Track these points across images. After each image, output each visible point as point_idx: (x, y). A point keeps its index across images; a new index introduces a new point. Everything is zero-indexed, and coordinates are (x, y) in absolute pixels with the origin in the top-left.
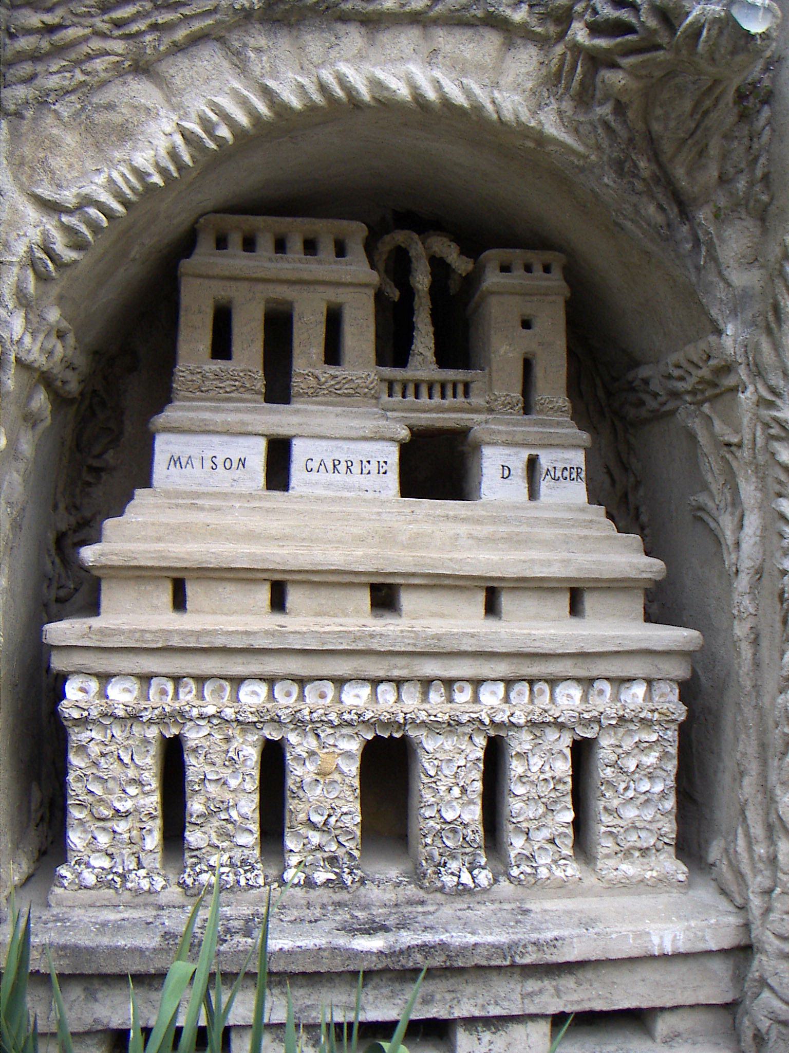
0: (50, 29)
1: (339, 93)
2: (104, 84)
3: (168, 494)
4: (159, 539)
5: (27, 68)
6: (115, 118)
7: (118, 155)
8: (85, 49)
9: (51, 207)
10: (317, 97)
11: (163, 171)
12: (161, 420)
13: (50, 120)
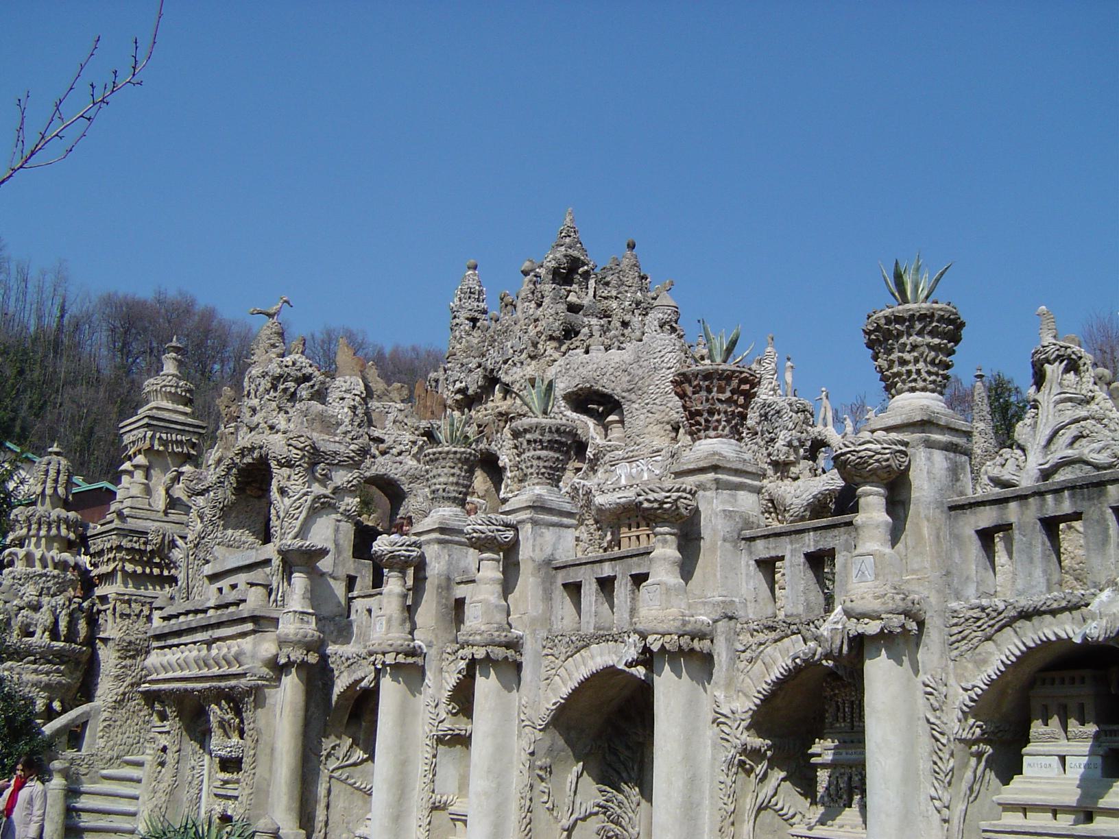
0: (960, 632)
1: (1045, 639)
2: (977, 647)
3: (1027, 777)
4: (1017, 794)
5: (956, 645)
6: (981, 657)
7: (983, 669)
8: (971, 636)
9: (966, 690)
10: (1039, 642)
11: (996, 674)
12: (1024, 750)
13: (964, 660)
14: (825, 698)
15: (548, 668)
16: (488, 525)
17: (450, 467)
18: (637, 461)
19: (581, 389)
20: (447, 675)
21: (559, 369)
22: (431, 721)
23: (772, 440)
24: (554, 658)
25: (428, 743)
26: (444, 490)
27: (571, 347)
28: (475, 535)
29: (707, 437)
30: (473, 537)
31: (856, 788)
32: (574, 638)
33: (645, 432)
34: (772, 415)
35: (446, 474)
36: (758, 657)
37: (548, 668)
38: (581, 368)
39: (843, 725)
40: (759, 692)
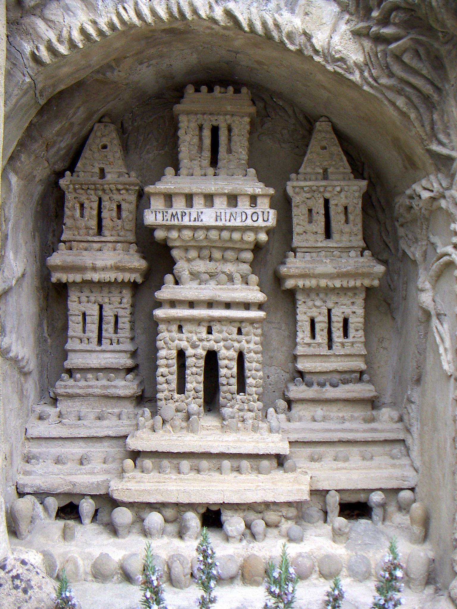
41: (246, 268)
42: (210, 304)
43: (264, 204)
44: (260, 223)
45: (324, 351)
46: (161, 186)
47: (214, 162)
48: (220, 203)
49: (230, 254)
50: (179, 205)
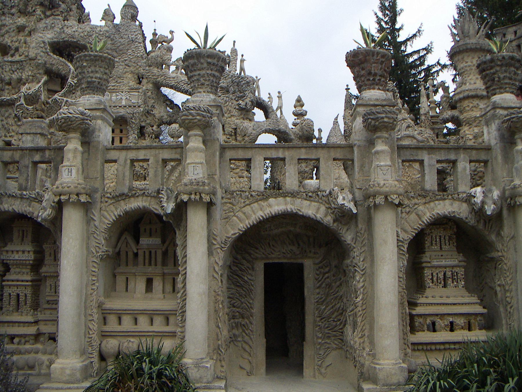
14: (426, 234)
15: (227, 212)
16: (206, 112)
17: (105, 68)
18: (118, 92)
19: (65, 41)
20: (106, 213)
21: (45, 25)
22: (97, 245)
23: (241, 97)
24: (231, 206)
25: (95, 260)
26: (99, 83)
27: (55, 14)
28: (198, 117)
29: (379, 89)
30: (196, 119)
31: (449, 278)
32: (253, 193)
33: (124, 76)
34: (244, 84)
35: (102, 72)
36: (412, 212)
37: (227, 212)
38: (65, 28)
39: (436, 247)
40: (415, 229)
41: (29, 270)
42: (18, 281)
43: (31, 253)
44: (30, 258)
45: (53, 294)
46: (6, 249)
47: (23, 240)
48: (20, 253)
49: (24, 267)
50: (10, 253)
